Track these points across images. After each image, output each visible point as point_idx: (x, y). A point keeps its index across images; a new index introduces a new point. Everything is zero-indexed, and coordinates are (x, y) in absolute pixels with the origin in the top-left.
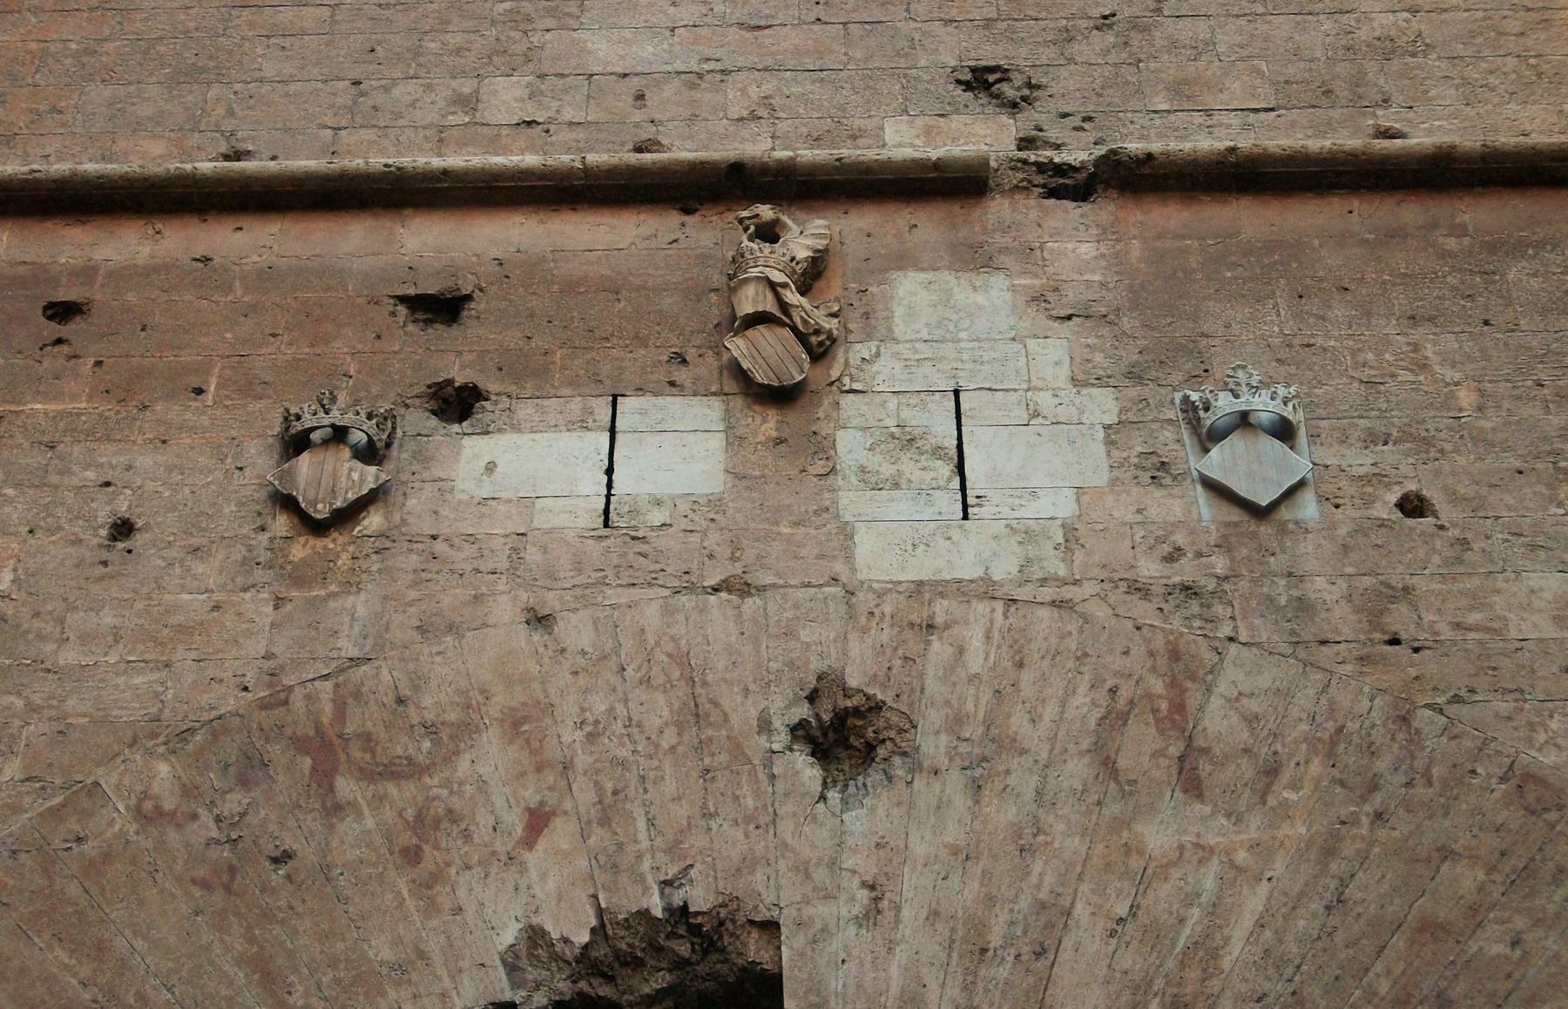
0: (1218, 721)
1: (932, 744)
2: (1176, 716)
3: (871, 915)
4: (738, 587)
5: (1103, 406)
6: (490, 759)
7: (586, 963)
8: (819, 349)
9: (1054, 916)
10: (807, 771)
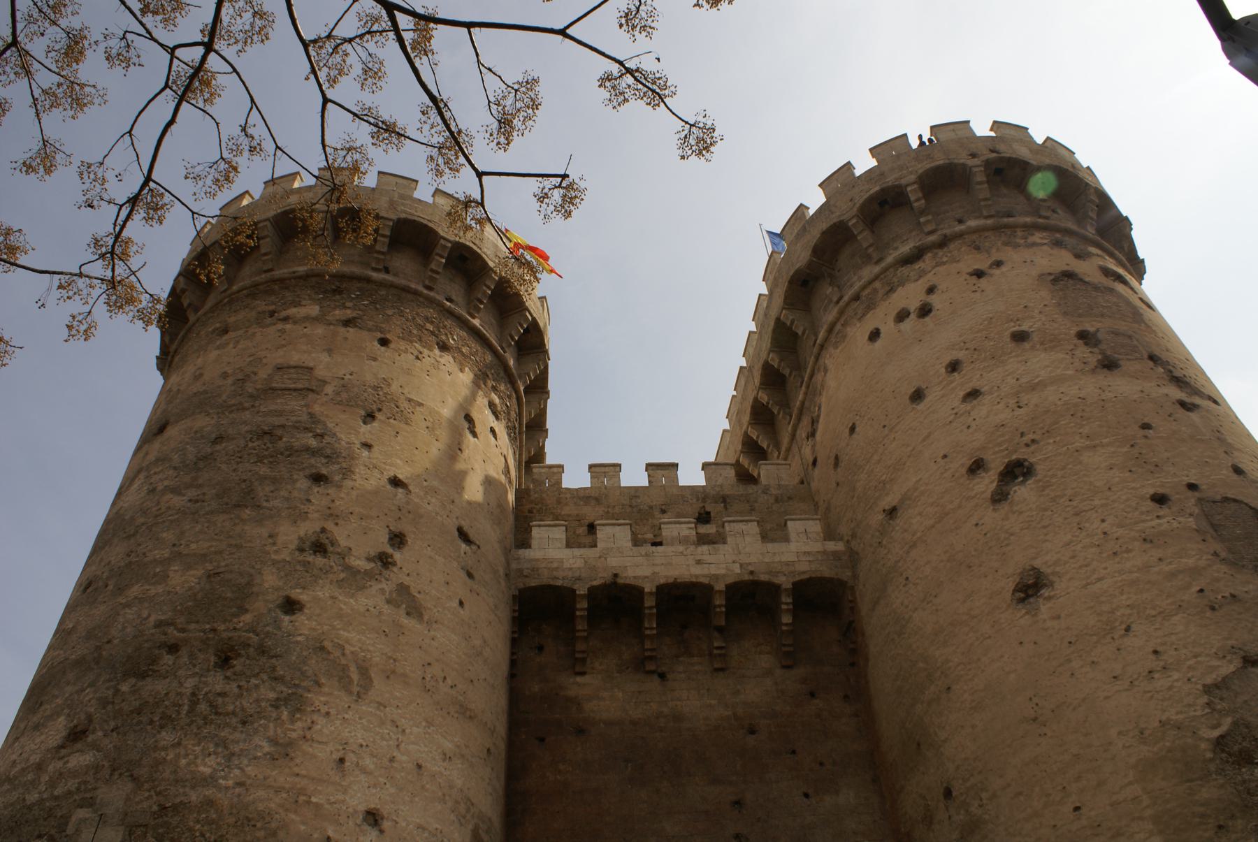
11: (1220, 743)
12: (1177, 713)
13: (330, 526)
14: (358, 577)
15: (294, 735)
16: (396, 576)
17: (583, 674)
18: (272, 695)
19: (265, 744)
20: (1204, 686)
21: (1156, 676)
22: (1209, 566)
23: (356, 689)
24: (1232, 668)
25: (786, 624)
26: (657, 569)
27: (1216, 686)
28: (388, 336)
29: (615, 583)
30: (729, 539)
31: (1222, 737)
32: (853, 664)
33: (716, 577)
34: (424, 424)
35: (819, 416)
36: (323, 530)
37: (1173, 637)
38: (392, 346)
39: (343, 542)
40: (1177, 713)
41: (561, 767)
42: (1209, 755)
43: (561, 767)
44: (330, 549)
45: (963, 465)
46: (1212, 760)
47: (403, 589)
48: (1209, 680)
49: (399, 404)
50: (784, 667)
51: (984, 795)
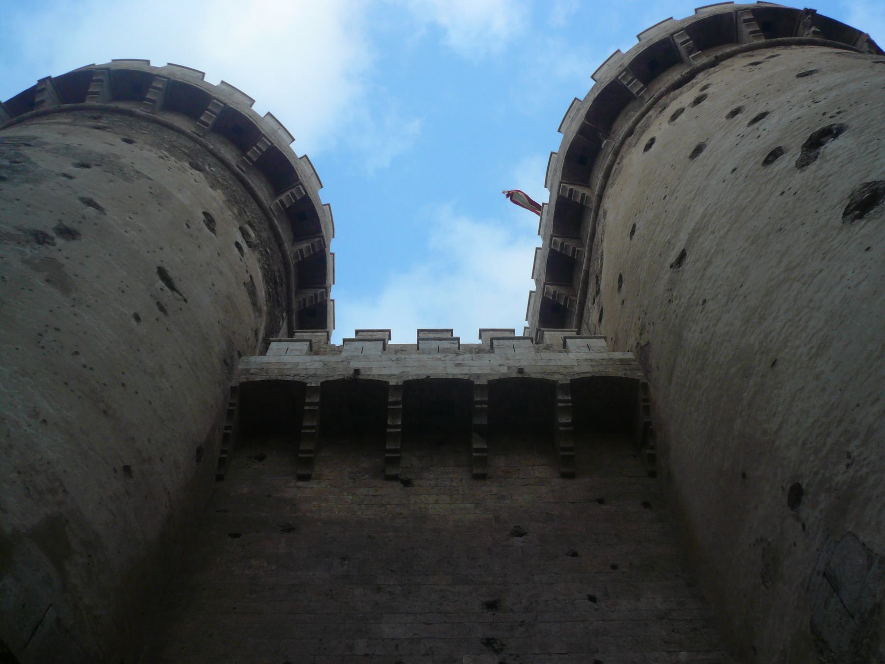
17: (306, 478)
25: (564, 425)
26: (408, 370)
29: (356, 380)
30: (496, 350)
32: (653, 474)
33: (478, 376)
35: (601, 272)
45: (756, 163)
50: (564, 476)
51: (852, 447)
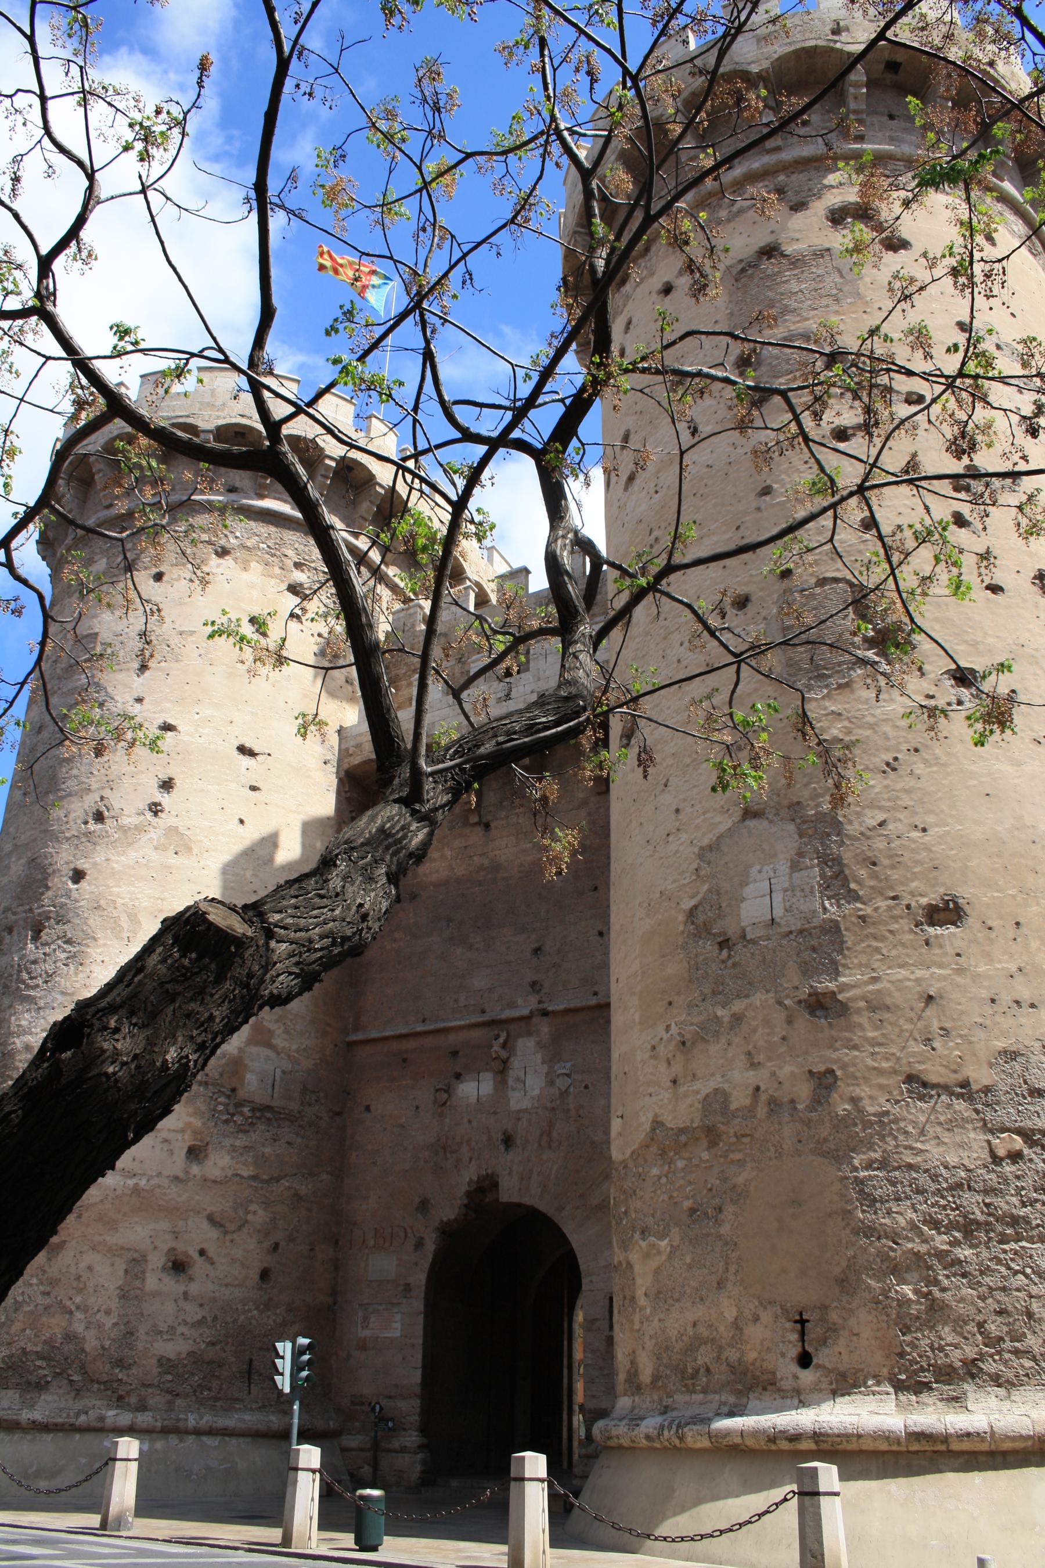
0: (555, 1135)
1: (518, 1142)
2: (549, 1134)
3: (510, 1173)
4: (495, 1113)
5: (545, 1068)
6: (465, 1149)
7: (478, 1182)
8: (505, 1062)
9: (531, 1171)
10: (502, 1148)
11: (692, 913)
12: (675, 881)
13: (107, 793)
14: (129, 834)
15: (78, 985)
16: (165, 820)
18: (63, 956)
19: (59, 996)
20: (702, 848)
21: (671, 839)
22: (756, 690)
23: (125, 935)
24: (729, 824)
27: (710, 848)
28: (162, 569)
31: (696, 907)
34: (197, 652)
36: (102, 798)
37: (695, 790)
38: (165, 578)
39: (117, 805)
40: (675, 881)
41: (397, 935)
42: (681, 928)
43: (397, 935)
44: (106, 814)
46: (683, 932)
47: (173, 830)
48: (706, 841)
49: (171, 643)
